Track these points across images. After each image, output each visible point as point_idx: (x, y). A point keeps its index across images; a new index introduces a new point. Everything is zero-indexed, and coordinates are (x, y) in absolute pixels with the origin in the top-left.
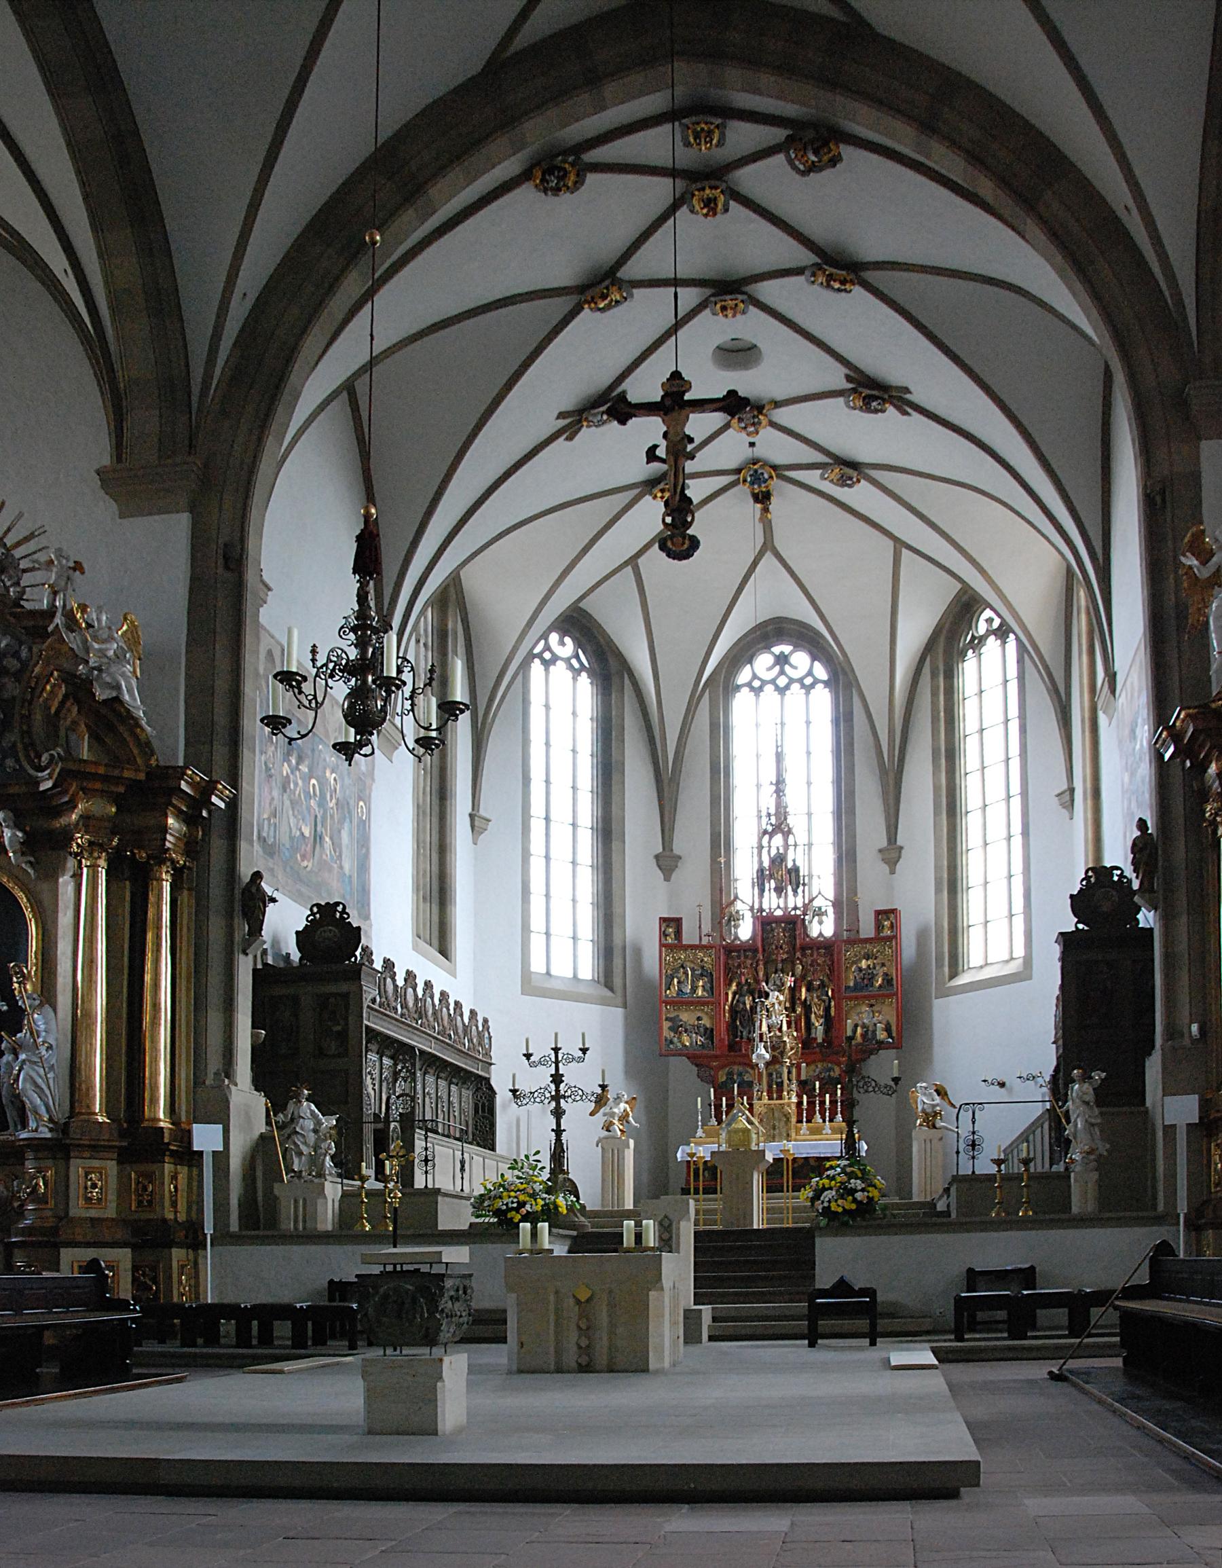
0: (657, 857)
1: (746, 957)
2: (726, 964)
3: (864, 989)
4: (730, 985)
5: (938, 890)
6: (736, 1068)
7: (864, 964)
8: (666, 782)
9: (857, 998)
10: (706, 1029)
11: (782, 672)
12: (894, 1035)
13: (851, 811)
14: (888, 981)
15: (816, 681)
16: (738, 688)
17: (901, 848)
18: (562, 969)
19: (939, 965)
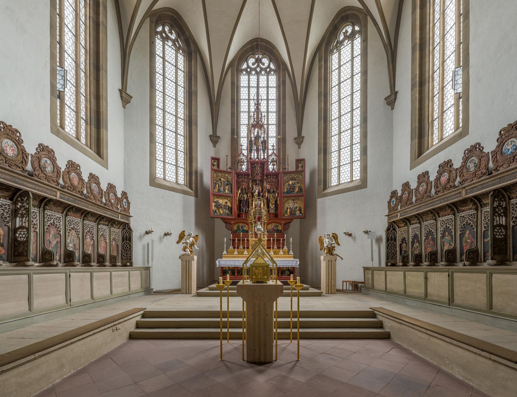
0: (210, 136)
1: (245, 178)
2: (237, 180)
3: (290, 194)
4: (238, 189)
5: (319, 153)
6: (241, 224)
7: (291, 182)
8: (214, 104)
9: (287, 197)
10: (229, 207)
11: (258, 66)
12: (303, 212)
13: (284, 122)
14: (300, 190)
15: (271, 70)
16: (242, 71)
17: (303, 137)
19: (319, 184)
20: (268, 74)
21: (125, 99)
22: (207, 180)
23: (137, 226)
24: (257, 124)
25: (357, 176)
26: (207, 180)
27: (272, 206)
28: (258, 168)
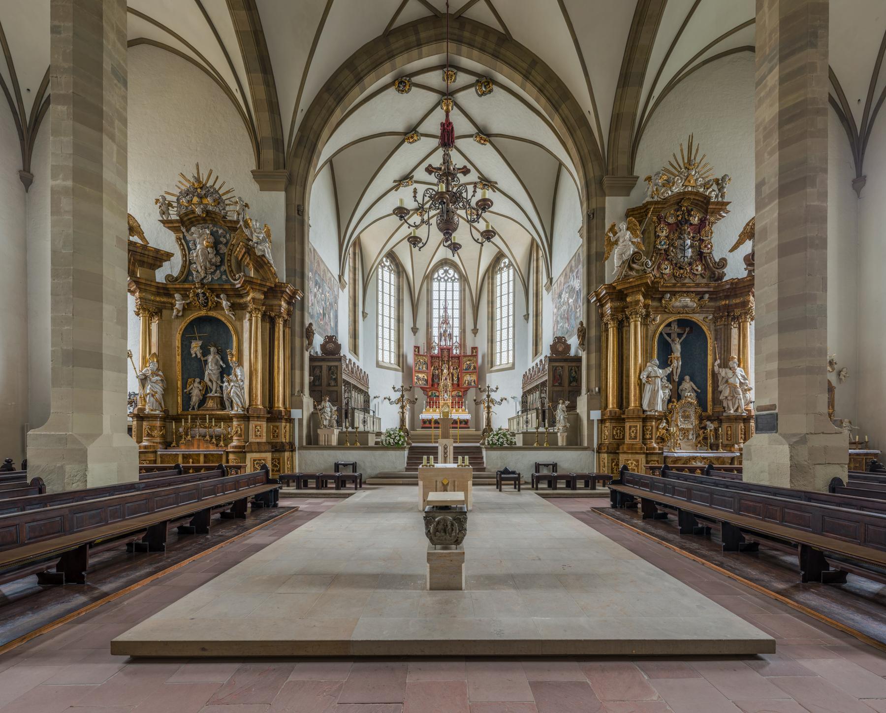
13: (465, 318)
14: (475, 368)
20: (453, 281)
21: (365, 315)
22: (410, 359)
23: (372, 393)
24: (445, 321)
25: (511, 361)
26: (410, 359)
27: (455, 379)
28: (446, 353)
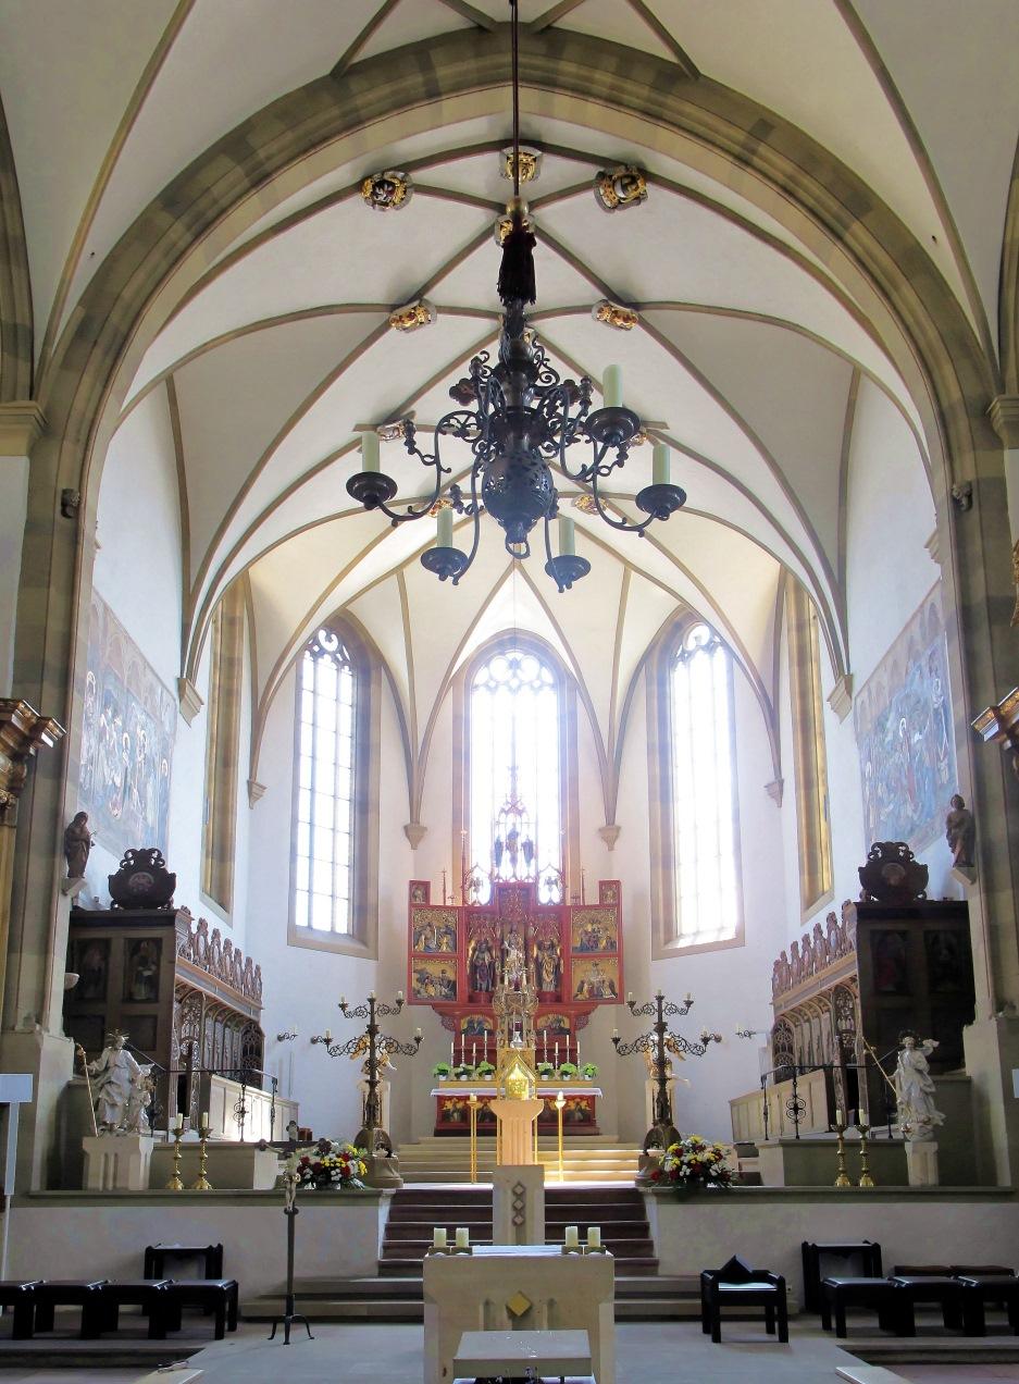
6: (477, 1017)
12: (617, 991)
18: (322, 924)
27: (548, 978)
